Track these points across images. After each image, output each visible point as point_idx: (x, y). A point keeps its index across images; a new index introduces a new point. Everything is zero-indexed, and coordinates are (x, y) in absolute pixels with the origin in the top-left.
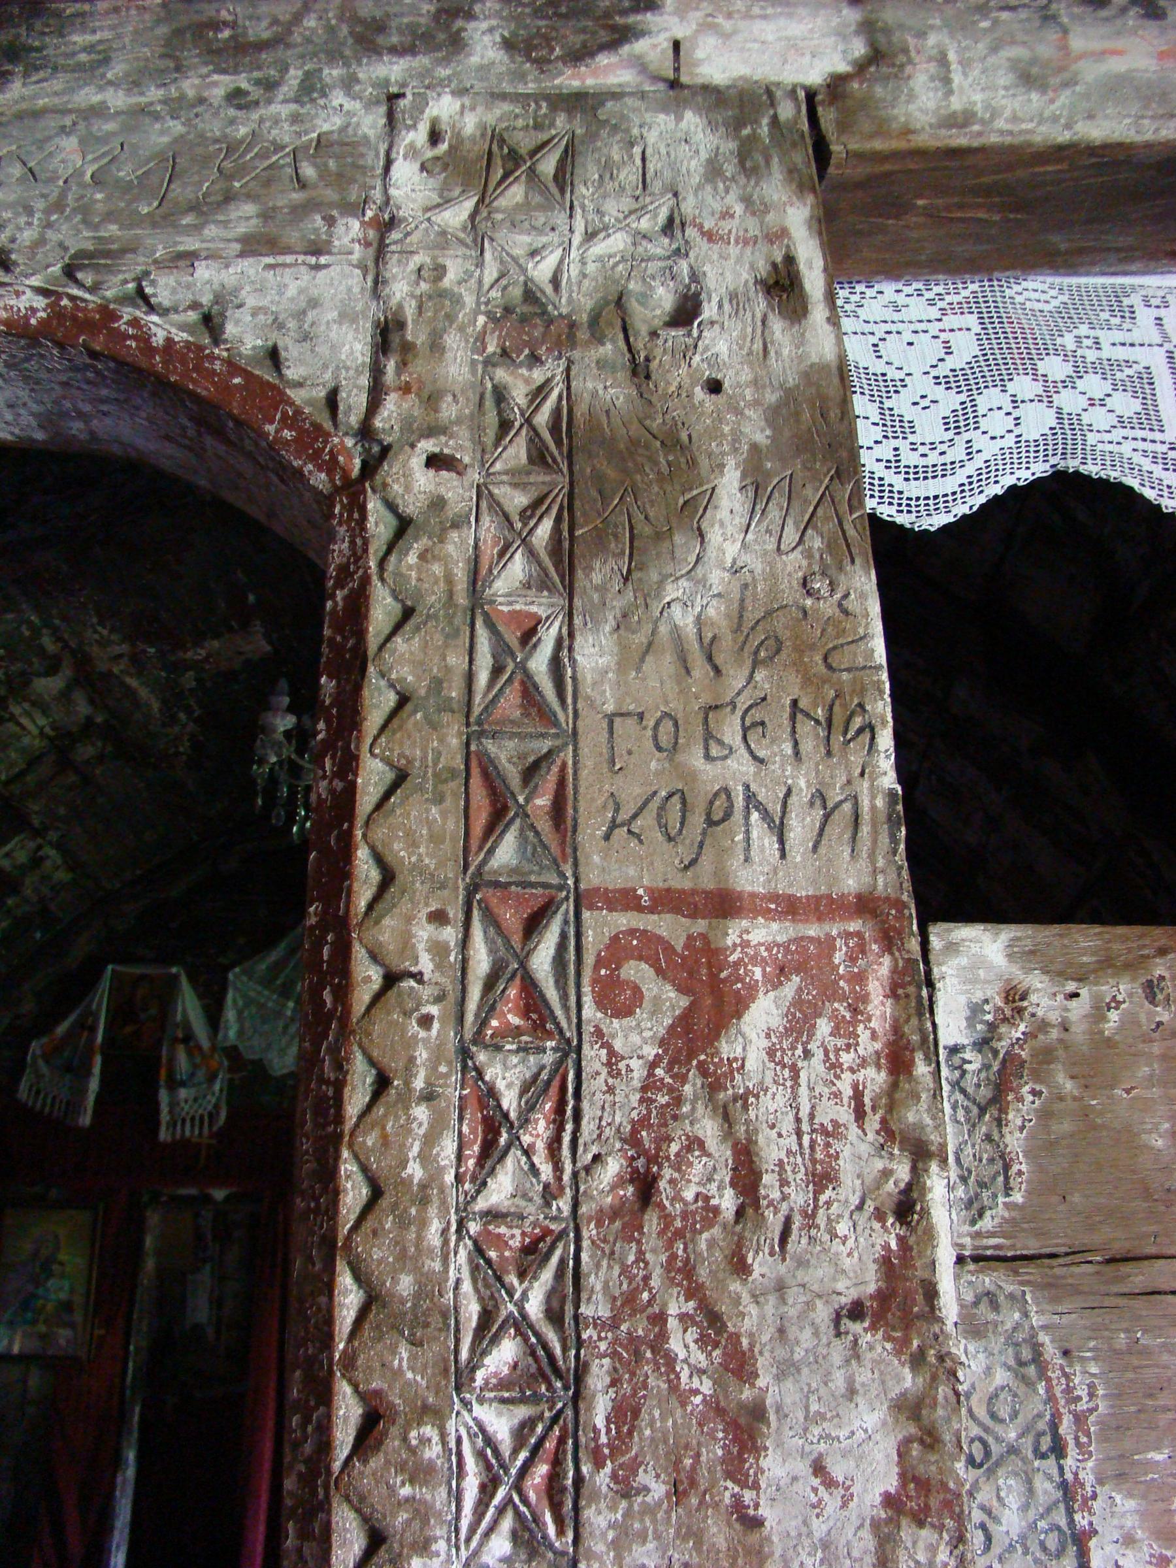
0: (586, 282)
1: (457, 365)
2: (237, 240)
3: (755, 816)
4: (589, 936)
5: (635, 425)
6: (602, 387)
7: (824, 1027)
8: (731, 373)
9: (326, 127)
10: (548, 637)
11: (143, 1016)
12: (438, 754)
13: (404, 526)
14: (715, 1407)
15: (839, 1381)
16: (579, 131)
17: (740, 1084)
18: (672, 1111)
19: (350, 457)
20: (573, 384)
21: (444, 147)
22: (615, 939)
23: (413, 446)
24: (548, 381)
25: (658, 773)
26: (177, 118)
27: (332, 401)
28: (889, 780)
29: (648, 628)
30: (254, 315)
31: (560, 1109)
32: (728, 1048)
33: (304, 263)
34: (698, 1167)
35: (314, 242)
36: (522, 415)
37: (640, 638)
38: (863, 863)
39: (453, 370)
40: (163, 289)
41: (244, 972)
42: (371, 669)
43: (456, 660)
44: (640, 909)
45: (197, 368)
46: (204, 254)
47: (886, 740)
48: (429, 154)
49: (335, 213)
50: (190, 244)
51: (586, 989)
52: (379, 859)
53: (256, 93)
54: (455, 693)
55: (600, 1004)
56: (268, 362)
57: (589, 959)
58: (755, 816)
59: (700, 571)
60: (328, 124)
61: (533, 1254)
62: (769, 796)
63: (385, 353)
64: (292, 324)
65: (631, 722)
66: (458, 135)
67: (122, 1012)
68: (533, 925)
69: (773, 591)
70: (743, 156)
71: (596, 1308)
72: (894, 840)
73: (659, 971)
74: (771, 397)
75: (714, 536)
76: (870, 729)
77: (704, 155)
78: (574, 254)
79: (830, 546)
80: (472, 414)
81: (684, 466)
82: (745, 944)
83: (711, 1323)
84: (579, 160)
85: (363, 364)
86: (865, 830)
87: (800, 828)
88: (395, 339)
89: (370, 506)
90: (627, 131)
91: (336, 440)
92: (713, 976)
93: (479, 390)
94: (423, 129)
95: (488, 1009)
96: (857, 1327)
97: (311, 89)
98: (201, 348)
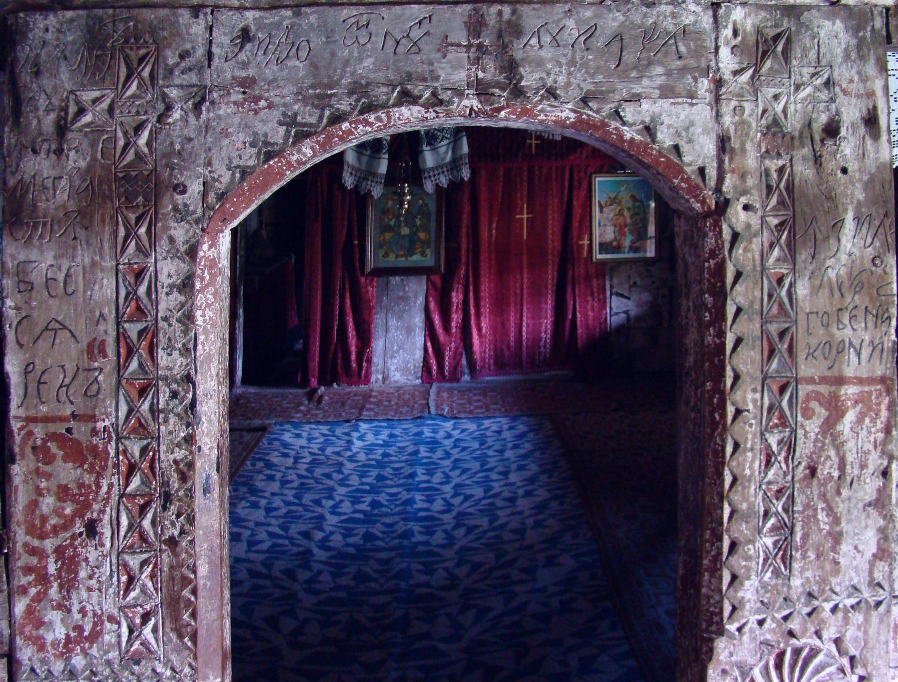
0: (797, 115)
1: (751, 160)
2: (657, 88)
3: (852, 350)
4: (800, 393)
5: (816, 188)
6: (804, 170)
7: (867, 420)
8: (851, 164)
9: (687, 22)
10: (787, 282)
12: (753, 331)
13: (736, 236)
14: (829, 533)
15: (863, 524)
16: (793, 29)
17: (842, 438)
18: (822, 449)
19: (711, 199)
21: (739, 39)
22: (808, 394)
23: (738, 200)
24: (784, 166)
25: (823, 335)
26: (619, 11)
27: (702, 171)
28: (893, 337)
29: (820, 278)
30: (668, 128)
31: (789, 449)
32: (839, 427)
33: (687, 103)
34: (828, 463)
35: (689, 91)
37: (817, 283)
38: (883, 366)
40: (629, 112)
42: (729, 298)
43: (757, 293)
44: (815, 383)
45: (644, 151)
46: (644, 95)
47: (894, 323)
48: (734, 43)
49: (697, 75)
50: (637, 89)
51: (799, 411)
52: (734, 370)
54: (757, 307)
55: (803, 416)
56: (674, 151)
57: (800, 401)
58: (852, 350)
59: (838, 255)
60: (688, 20)
61: (780, 492)
62: (856, 342)
63: (724, 153)
64: (684, 134)
65: (814, 315)
66: (744, 31)
68: (782, 389)
69: (862, 264)
70: (859, 47)
71: (798, 508)
72: (893, 357)
73: (820, 404)
74: (865, 178)
75: (844, 241)
76: (889, 318)
77: (843, 46)
78: (792, 98)
79: (882, 246)
82: (846, 394)
83: (830, 510)
84: (793, 46)
86: (885, 354)
87: (865, 354)
88: (727, 145)
90: (812, 30)
92: (836, 405)
94: (730, 27)
95: (769, 419)
96: (869, 509)
98: (648, 144)
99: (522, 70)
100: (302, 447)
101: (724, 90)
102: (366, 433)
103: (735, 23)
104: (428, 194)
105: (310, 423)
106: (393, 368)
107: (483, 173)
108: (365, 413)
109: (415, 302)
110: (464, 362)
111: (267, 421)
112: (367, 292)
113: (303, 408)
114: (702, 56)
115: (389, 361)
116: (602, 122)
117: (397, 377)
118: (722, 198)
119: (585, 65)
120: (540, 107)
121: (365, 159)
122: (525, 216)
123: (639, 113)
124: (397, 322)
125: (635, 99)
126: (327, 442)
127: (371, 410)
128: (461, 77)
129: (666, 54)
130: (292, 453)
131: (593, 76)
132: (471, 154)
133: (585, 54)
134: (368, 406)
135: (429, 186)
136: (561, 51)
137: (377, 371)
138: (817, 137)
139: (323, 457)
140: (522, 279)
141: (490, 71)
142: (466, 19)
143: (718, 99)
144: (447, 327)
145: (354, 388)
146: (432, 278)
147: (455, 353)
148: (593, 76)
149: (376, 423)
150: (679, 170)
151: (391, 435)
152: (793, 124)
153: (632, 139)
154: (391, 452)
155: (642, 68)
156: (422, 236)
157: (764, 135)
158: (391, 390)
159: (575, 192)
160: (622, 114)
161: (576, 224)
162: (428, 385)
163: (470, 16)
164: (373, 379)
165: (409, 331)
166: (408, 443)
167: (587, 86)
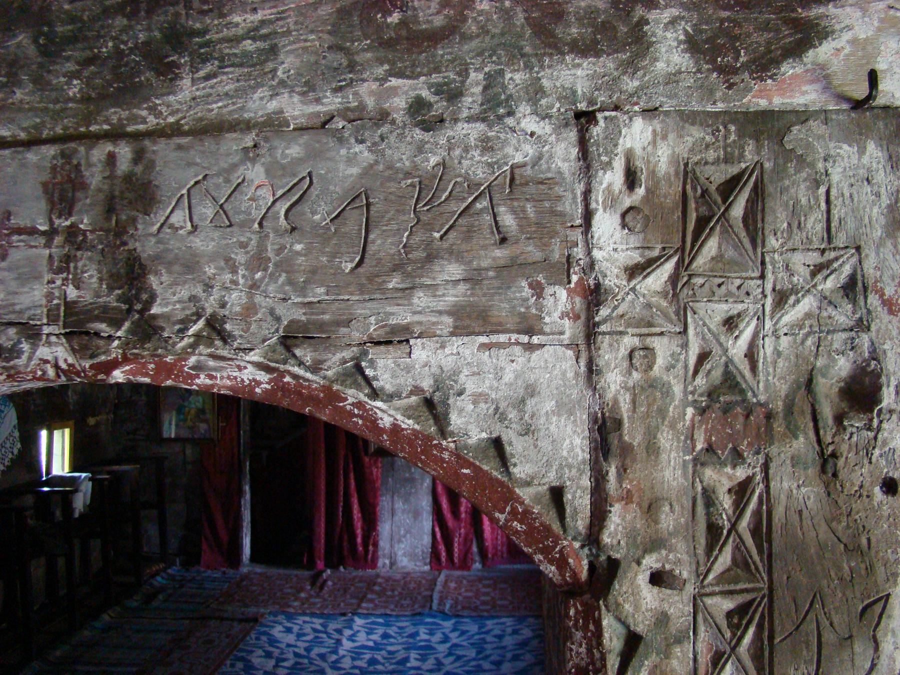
0: (781, 363)
2: (449, 313)
5: (823, 528)
6: (794, 488)
9: (518, 158)
16: (768, 165)
19: (578, 559)
20: (772, 484)
21: (641, 191)
23: (639, 563)
24: (749, 480)
26: (362, 142)
27: (557, 494)
30: (475, 403)
33: (518, 343)
35: (523, 317)
36: (729, 520)
39: (668, 474)
40: (384, 369)
46: (417, 330)
48: (627, 202)
49: (540, 278)
50: (401, 316)
53: (440, 106)
56: (492, 452)
60: (519, 153)
63: (606, 459)
64: (512, 415)
66: (653, 173)
77: (885, 201)
78: (768, 324)
80: (687, 524)
81: (863, 572)
84: (769, 204)
85: (584, 462)
88: (614, 441)
89: (605, 623)
90: (812, 165)
91: (565, 543)
93: (691, 494)
94: (619, 165)
97: (496, 107)
98: (428, 438)
99: (153, 280)
100: (289, 645)
101: (604, 312)
102: (358, 631)
103: (629, 157)
105: (305, 614)
106: (400, 553)
109: (422, 484)
110: (475, 549)
111: (262, 610)
113: (303, 595)
114: (553, 234)
115: (396, 546)
116: (327, 389)
117: (405, 562)
118: (603, 558)
119: (286, 265)
120: (193, 360)
123: (408, 369)
125: (397, 338)
126: (317, 641)
127: (371, 601)
128: (34, 297)
129: (469, 234)
130: (276, 652)
131: (302, 290)
133: (287, 240)
134: (369, 596)
136: (238, 236)
137: (384, 556)
138: (827, 412)
139: (306, 661)
141: (89, 286)
142: (46, 176)
143: (591, 333)
144: (455, 512)
145: (360, 573)
147: (465, 539)
148: (302, 290)
149: (373, 619)
150: (507, 496)
151: (385, 636)
152: (771, 384)
153: (396, 429)
154: (379, 658)
155: (413, 266)
157: (702, 411)
158: (398, 577)
160: (369, 372)
162: (437, 573)
163: (54, 168)
164: (380, 564)
165: (417, 514)
166: (400, 647)
167: (291, 313)
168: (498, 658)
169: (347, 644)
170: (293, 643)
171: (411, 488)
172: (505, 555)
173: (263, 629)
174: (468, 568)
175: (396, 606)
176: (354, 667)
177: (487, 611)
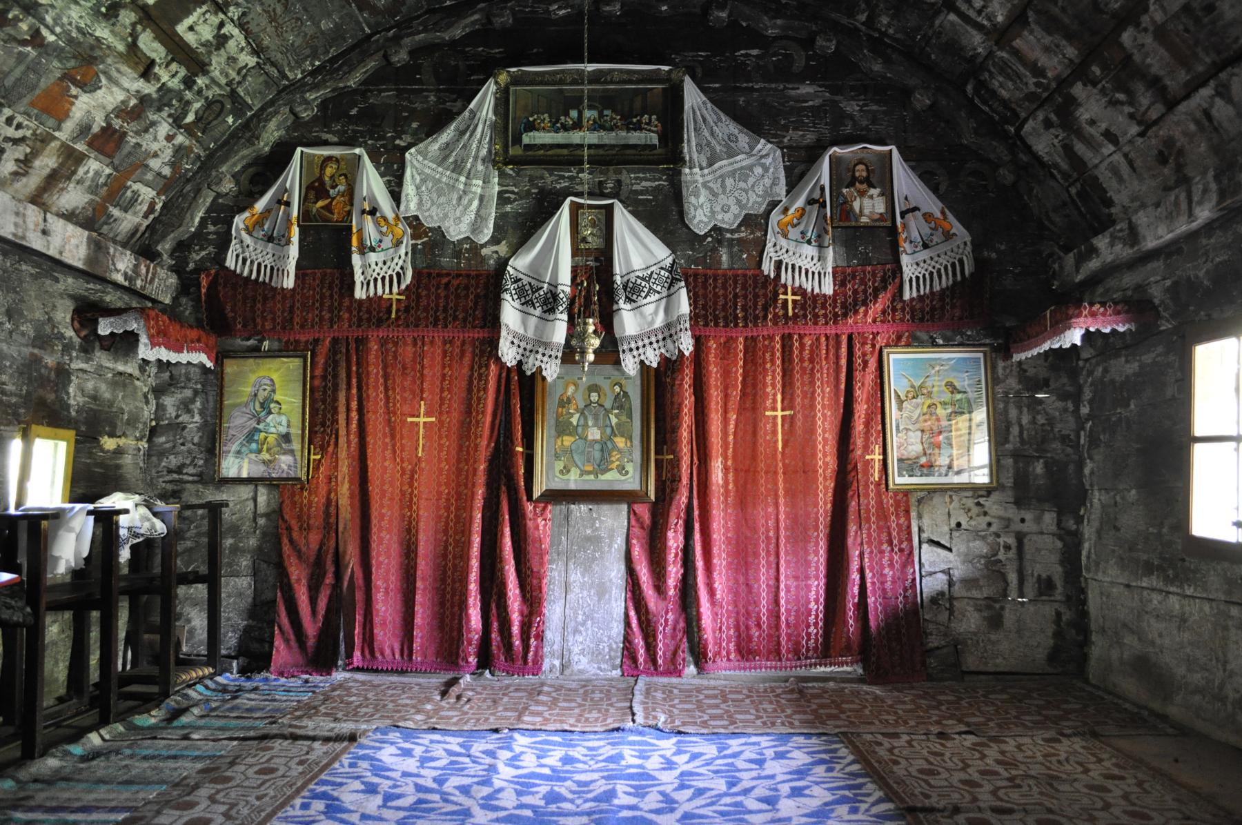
11: (331, 191)
41: (419, 152)
67: (315, 189)
100: (405, 774)
104: (628, 378)
106: (576, 650)
107: (712, 344)
108: (526, 718)
109: (610, 546)
111: (364, 726)
112: (537, 528)
115: (571, 638)
117: (583, 664)
121: (533, 321)
122: (779, 413)
124: (583, 576)
126: (454, 768)
127: (539, 714)
130: (385, 785)
132: (694, 317)
135: (630, 365)
139: (436, 797)
140: (777, 505)
144: (660, 588)
146: (637, 507)
149: (543, 737)
151: (567, 760)
154: (563, 791)
156: (620, 442)
158: (574, 685)
159: (858, 375)
161: (859, 426)
162: (632, 680)
164: (546, 666)
165: (602, 591)
166: (596, 776)
168: (768, 793)
169: (506, 772)
170: (415, 771)
171: (594, 551)
172: (732, 656)
173: (361, 752)
174: (679, 674)
175: (578, 721)
176: (522, 806)
177: (725, 727)
